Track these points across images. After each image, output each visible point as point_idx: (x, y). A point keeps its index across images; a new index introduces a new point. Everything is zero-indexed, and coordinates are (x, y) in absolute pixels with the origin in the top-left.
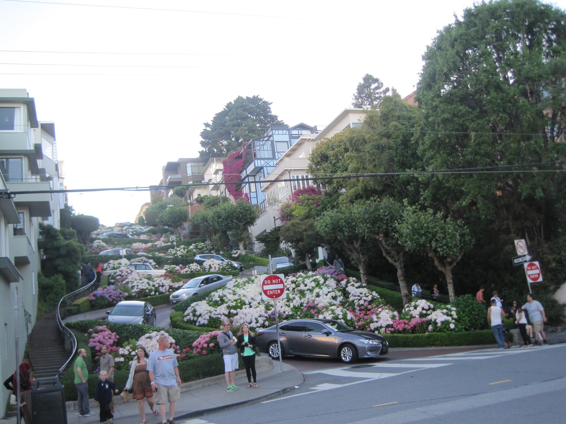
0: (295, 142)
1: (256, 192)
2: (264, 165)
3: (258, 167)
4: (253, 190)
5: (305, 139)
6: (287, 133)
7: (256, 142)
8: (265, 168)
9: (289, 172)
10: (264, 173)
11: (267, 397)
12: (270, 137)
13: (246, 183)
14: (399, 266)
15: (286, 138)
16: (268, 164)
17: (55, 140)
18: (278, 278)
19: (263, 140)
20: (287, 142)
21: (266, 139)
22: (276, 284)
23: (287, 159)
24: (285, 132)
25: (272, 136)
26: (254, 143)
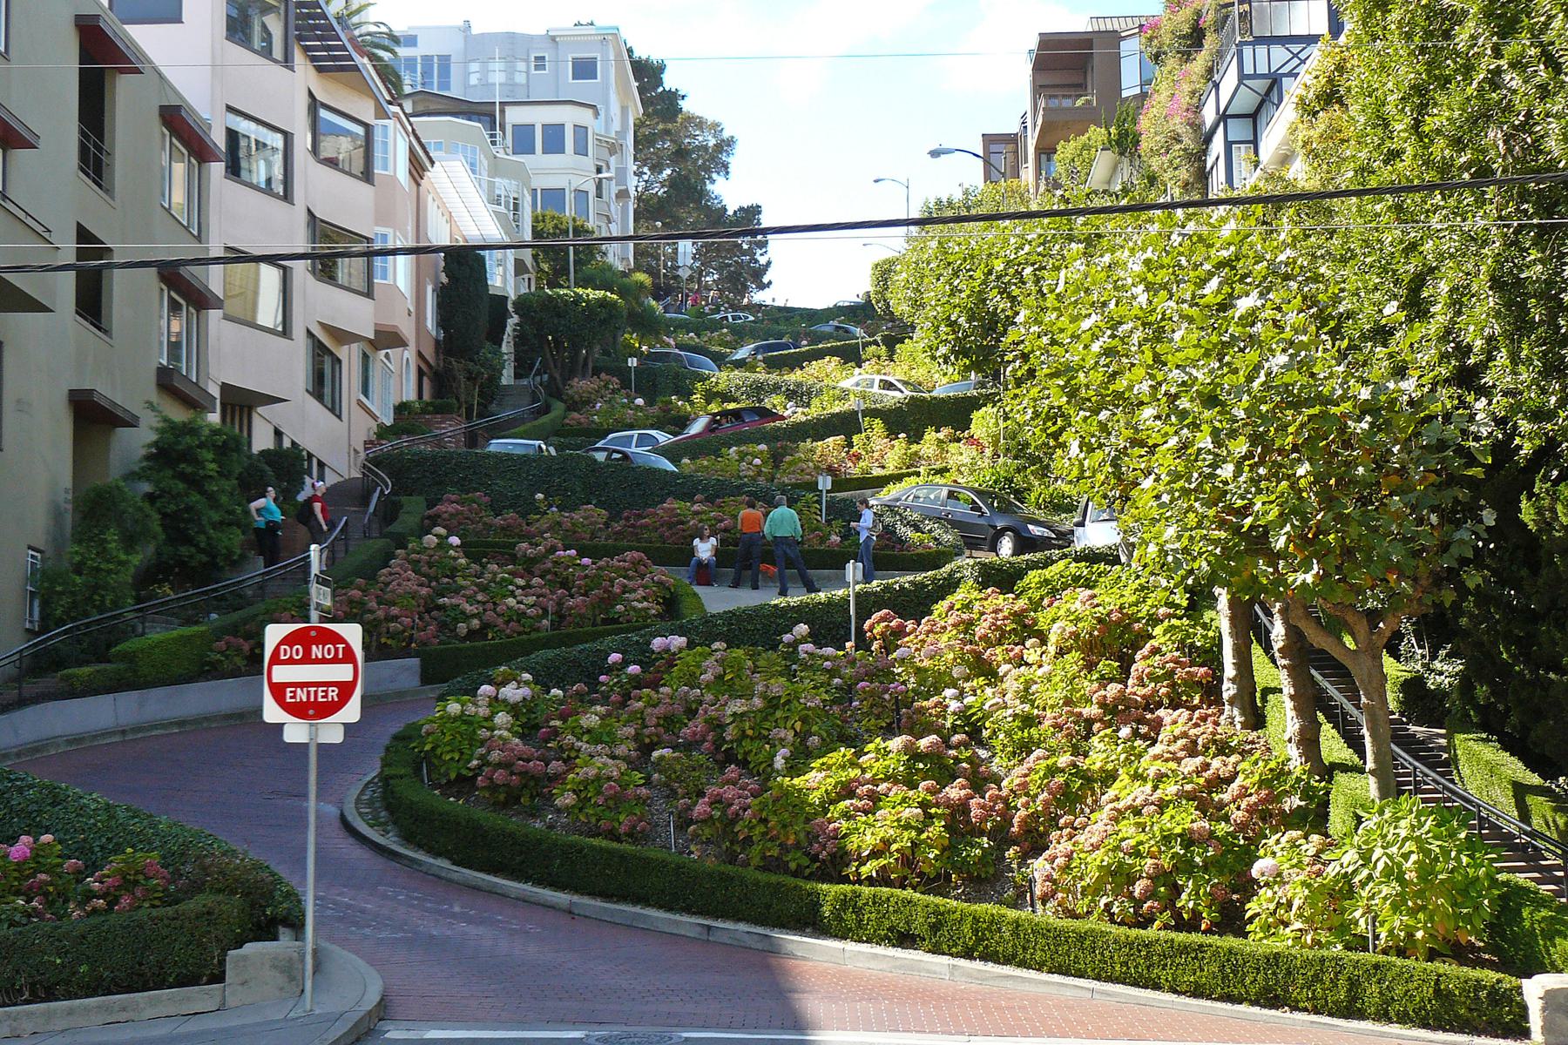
2: (1285, 70)
3: (1255, 76)
18: (336, 638)
22: (324, 661)
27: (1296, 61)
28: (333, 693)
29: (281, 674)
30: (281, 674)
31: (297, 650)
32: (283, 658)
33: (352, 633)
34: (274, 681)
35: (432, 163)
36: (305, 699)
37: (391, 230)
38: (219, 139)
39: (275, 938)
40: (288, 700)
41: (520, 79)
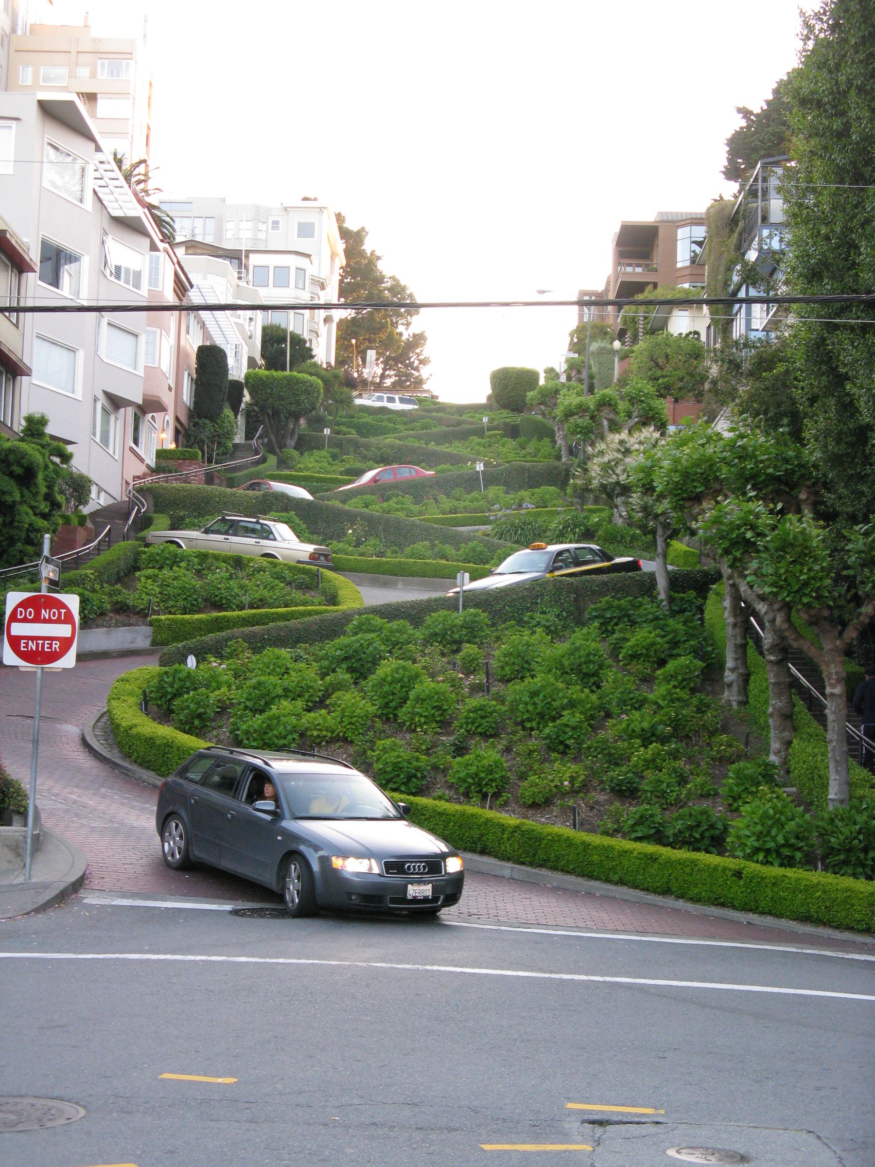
13: (741, 301)
18: (61, 605)
22: (49, 621)
28: (56, 645)
29: (18, 629)
30: (18, 629)
31: (30, 612)
32: (19, 617)
33: (72, 601)
35: (192, 286)
36: (34, 648)
37: (159, 330)
38: (34, 255)
39: (10, 824)
40: (22, 649)
41: (262, 236)
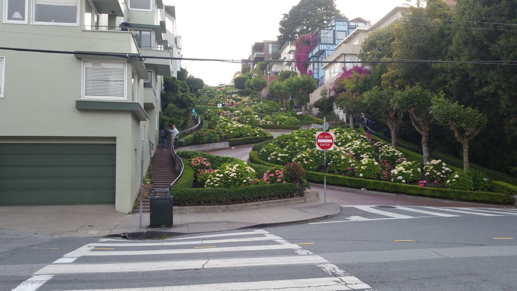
0: (352, 32)
1: (318, 69)
2: (326, 49)
3: (321, 50)
4: (316, 67)
5: (360, 30)
6: (347, 24)
7: (322, 30)
8: (327, 51)
9: (345, 56)
10: (325, 55)
11: (313, 220)
12: (333, 27)
14: (424, 135)
15: (345, 28)
16: (329, 48)
17: (175, 20)
18: (329, 135)
19: (327, 30)
20: (346, 31)
21: (330, 28)
22: (327, 139)
23: (344, 45)
24: (345, 23)
25: (334, 26)
26: (320, 31)
27: (328, 48)
29: (320, 141)
30: (320, 141)
34: (318, 142)
